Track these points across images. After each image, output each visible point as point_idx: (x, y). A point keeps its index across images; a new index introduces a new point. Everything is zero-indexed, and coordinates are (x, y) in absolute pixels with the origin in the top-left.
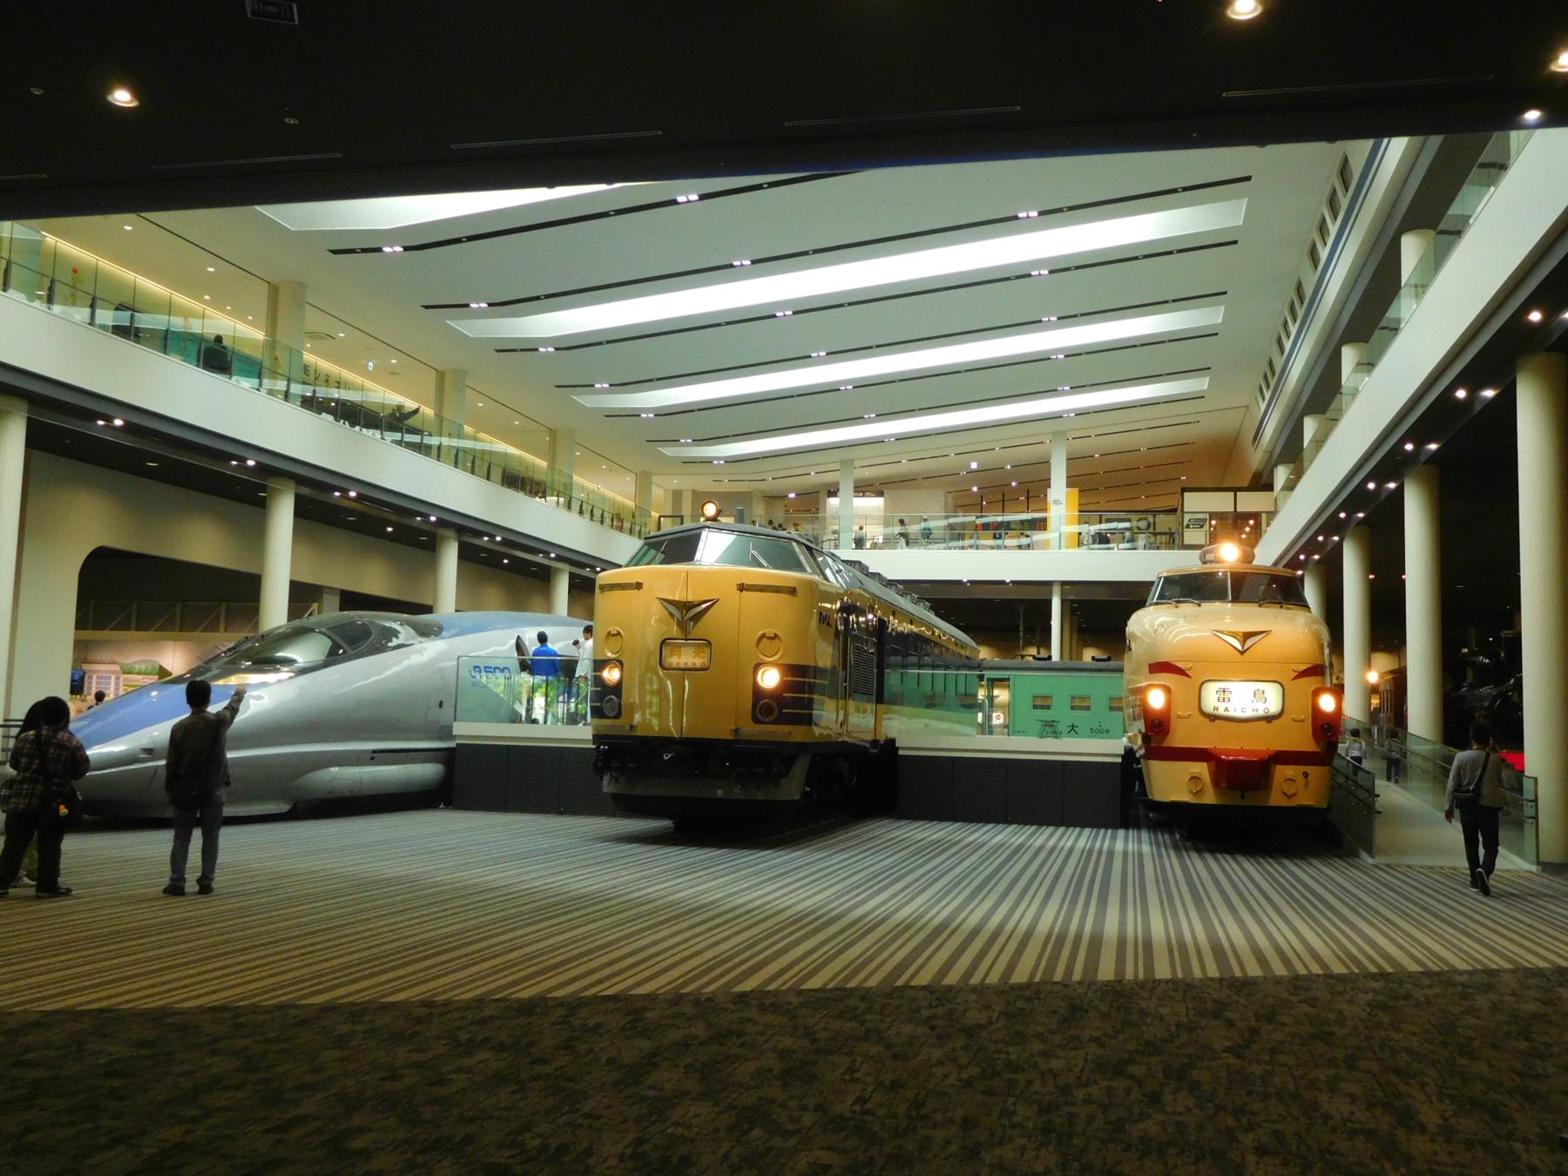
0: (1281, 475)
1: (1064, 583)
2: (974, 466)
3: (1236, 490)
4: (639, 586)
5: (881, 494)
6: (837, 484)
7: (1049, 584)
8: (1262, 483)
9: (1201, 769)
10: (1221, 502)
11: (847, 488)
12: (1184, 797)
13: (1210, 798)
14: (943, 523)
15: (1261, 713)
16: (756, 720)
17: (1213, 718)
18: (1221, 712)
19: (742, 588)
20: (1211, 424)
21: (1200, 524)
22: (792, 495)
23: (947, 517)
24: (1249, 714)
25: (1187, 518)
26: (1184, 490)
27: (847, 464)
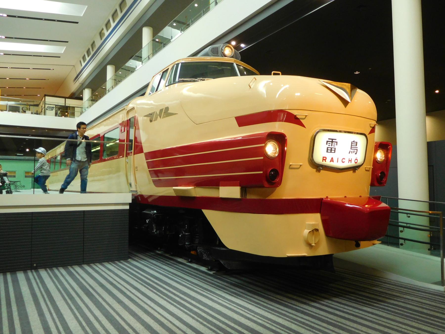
0: (87, 94)
3: (65, 98)
8: (78, 96)
9: (314, 220)
10: (60, 102)
12: (304, 252)
13: (323, 249)
15: (353, 164)
17: (318, 167)
18: (328, 163)
20: (57, 71)
21: (52, 109)
24: (346, 164)
25: (47, 106)
26: (45, 95)
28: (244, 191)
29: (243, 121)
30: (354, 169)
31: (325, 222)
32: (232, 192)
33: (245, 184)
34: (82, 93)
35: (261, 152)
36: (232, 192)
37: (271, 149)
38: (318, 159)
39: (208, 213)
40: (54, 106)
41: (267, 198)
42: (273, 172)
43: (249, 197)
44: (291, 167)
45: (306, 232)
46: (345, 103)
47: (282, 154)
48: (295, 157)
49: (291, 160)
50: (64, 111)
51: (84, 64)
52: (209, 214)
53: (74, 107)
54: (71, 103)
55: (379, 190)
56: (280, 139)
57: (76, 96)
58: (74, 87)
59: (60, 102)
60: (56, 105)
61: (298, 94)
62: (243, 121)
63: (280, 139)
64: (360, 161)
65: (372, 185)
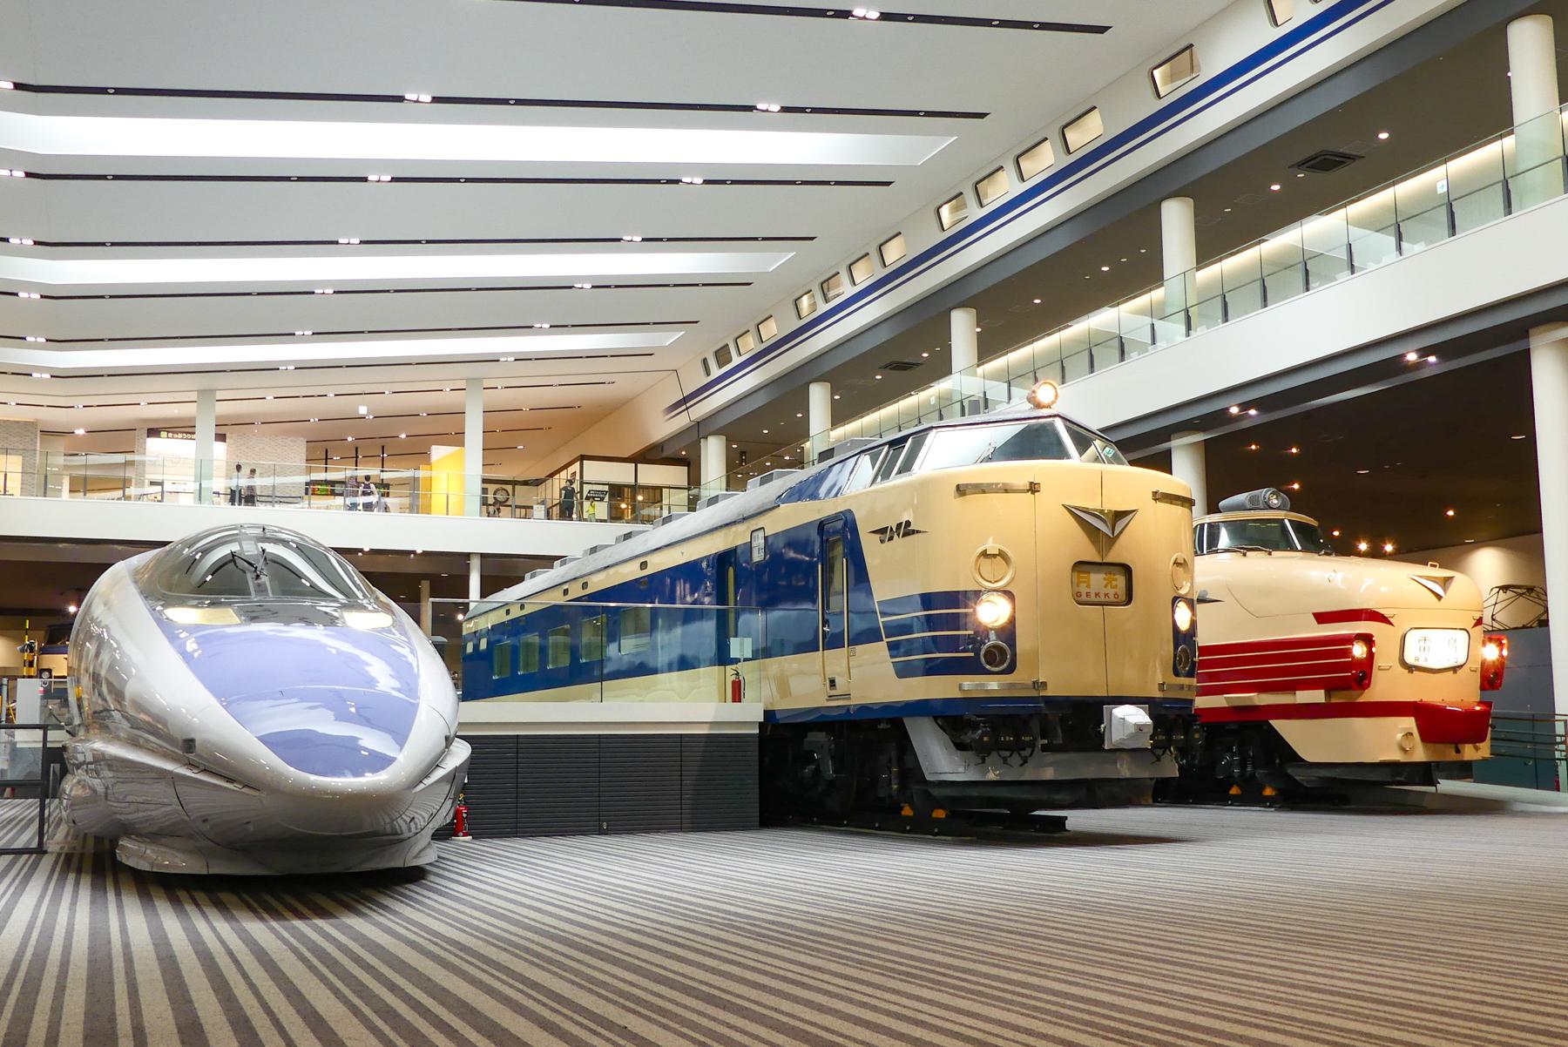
1: (483, 556)
2: (363, 411)
4: (1033, 488)
5: (221, 437)
6: (194, 419)
7: (468, 556)
9: (1409, 723)
11: (206, 429)
12: (1397, 756)
13: (1420, 754)
14: (305, 479)
15: (1452, 664)
16: (1177, 673)
17: (1411, 669)
18: (1421, 663)
19: (1159, 497)
22: (80, 432)
23: (309, 471)
25: (586, 488)
26: (582, 458)
27: (206, 394)
28: (1328, 695)
29: (1322, 618)
30: (1455, 669)
31: (1419, 726)
32: (1318, 696)
33: (1330, 687)
34: (695, 449)
35: (1347, 653)
36: (1318, 696)
37: (1359, 650)
38: (1410, 659)
39: (1276, 724)
40: (606, 488)
41: (1361, 700)
42: (1363, 673)
43: (1333, 701)
44: (1380, 668)
45: (1399, 736)
46: (1439, 597)
47: (1371, 655)
48: (1385, 656)
49: (1379, 662)
50: (625, 502)
51: (716, 372)
52: (1278, 724)
53: (660, 488)
54: (652, 475)
55: (1492, 695)
56: (1368, 640)
57: (666, 453)
58: (663, 428)
59: (622, 474)
60: (612, 486)
61: (1384, 589)
62: (1322, 618)
63: (1368, 640)
64: (1461, 661)
65: (1483, 688)
